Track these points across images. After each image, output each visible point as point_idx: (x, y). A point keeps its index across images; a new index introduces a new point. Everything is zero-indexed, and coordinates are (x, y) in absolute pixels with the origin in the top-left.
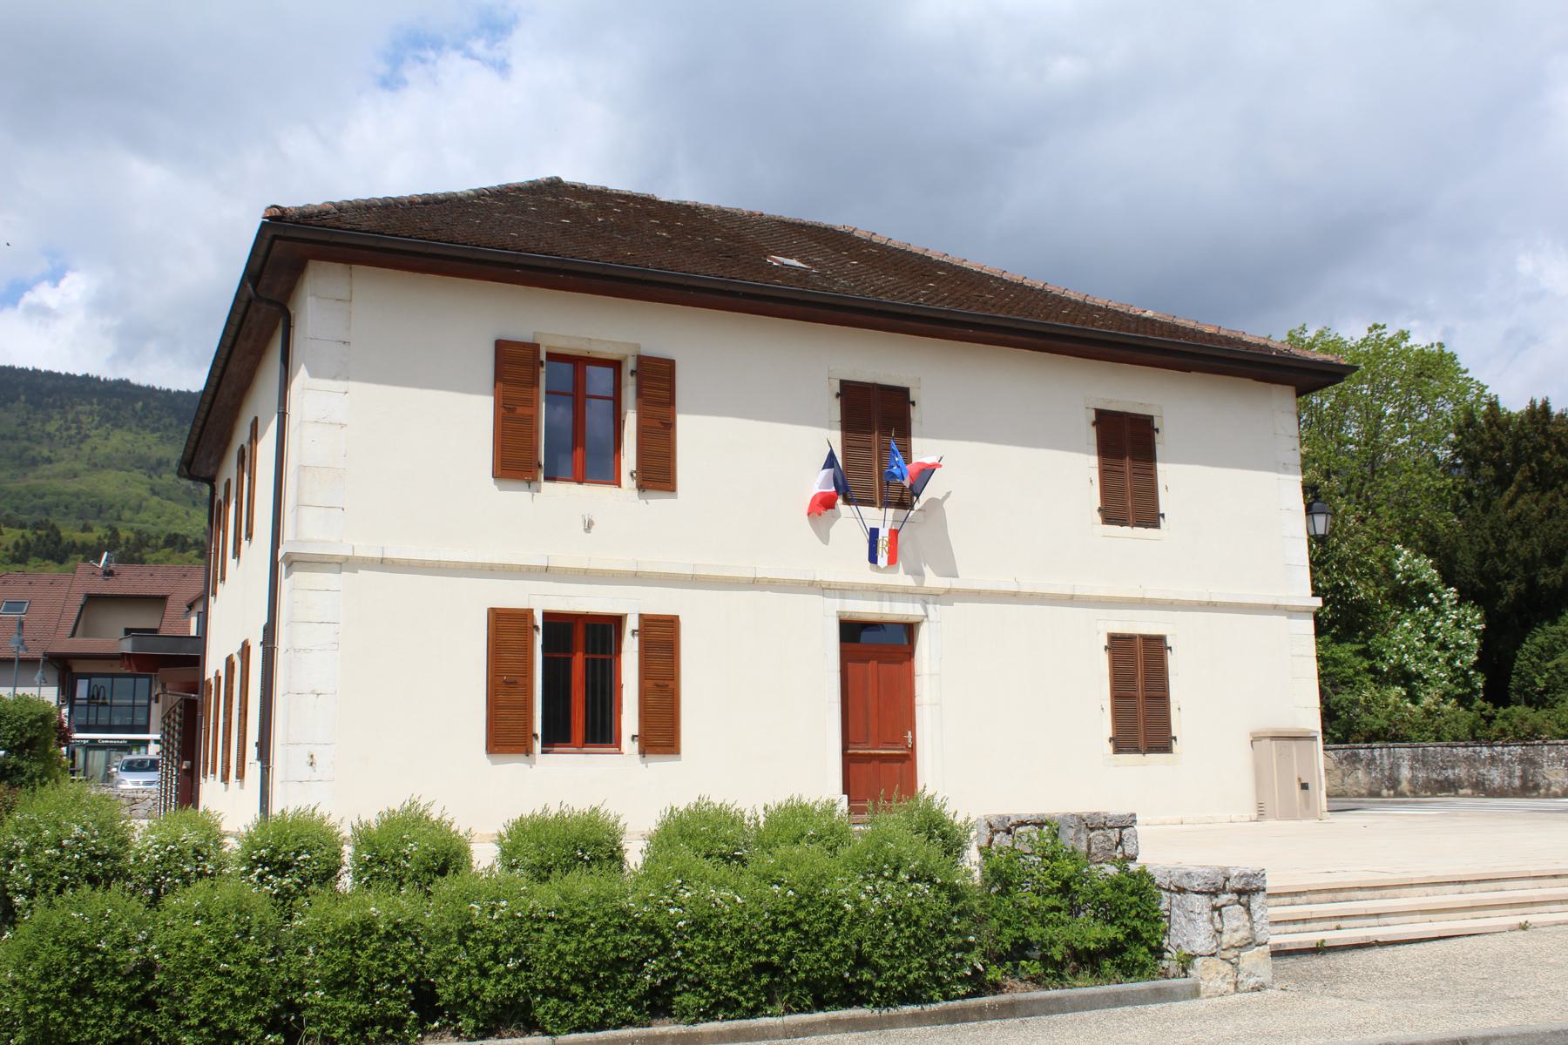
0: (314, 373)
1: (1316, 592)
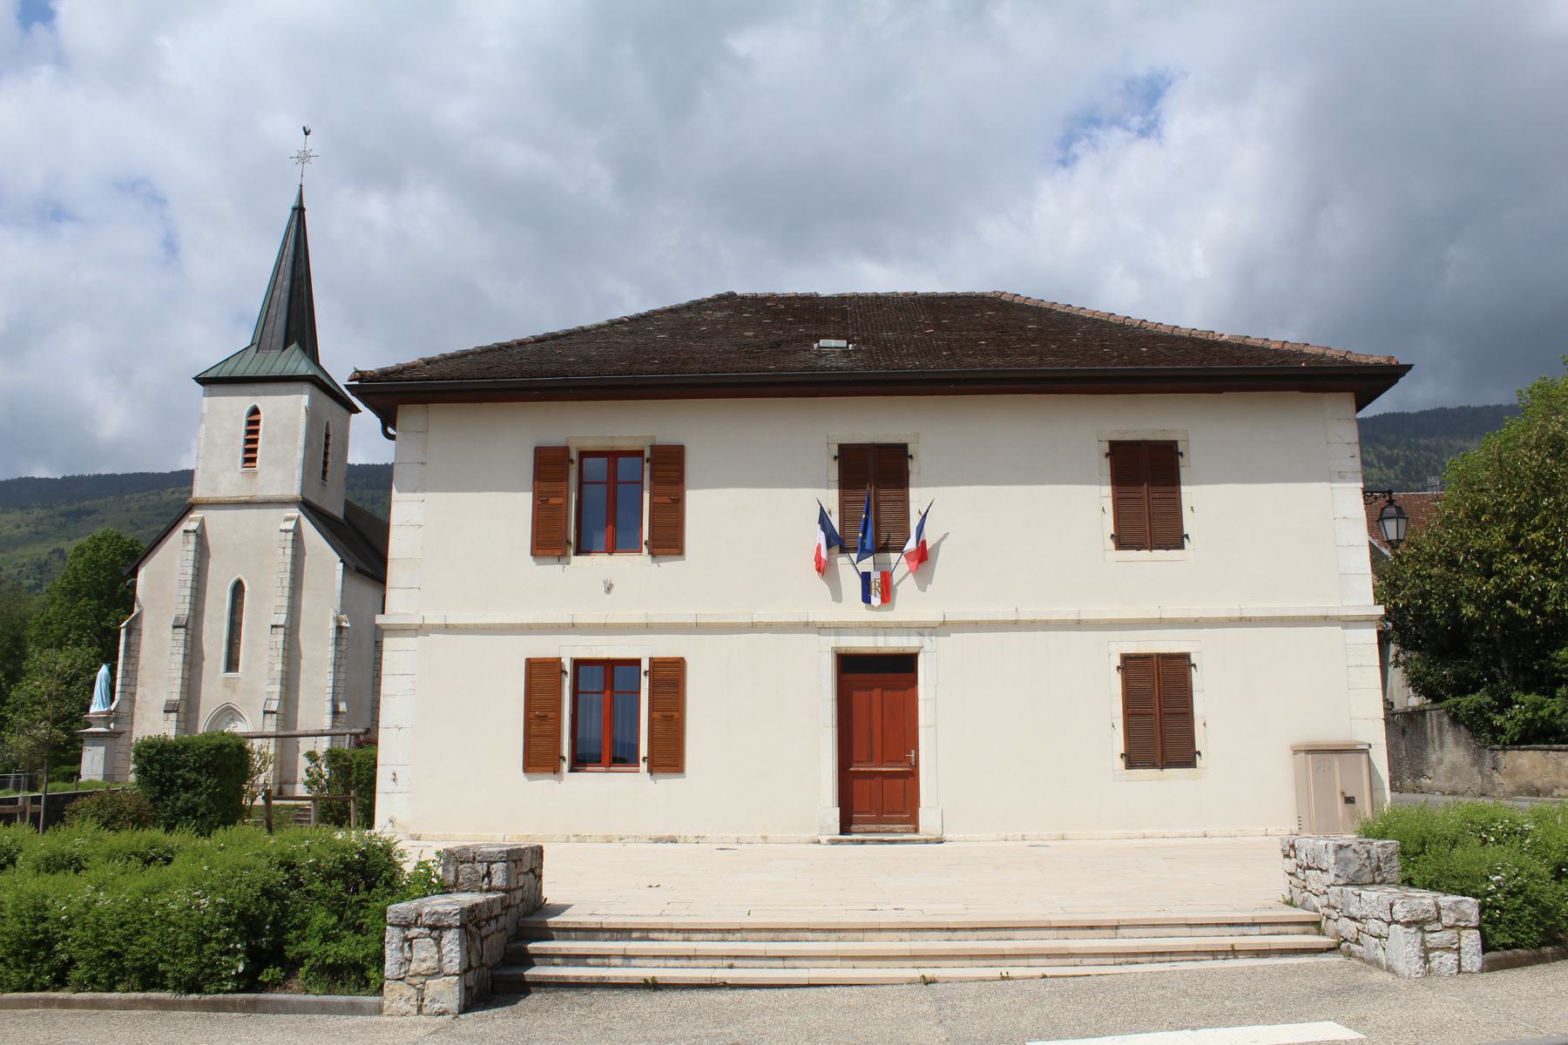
0: (399, 491)
1: (1379, 598)
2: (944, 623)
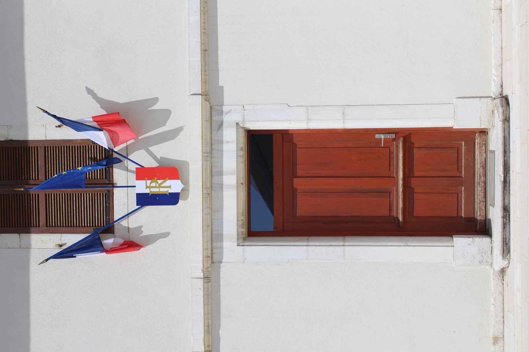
2: (205, 95)
